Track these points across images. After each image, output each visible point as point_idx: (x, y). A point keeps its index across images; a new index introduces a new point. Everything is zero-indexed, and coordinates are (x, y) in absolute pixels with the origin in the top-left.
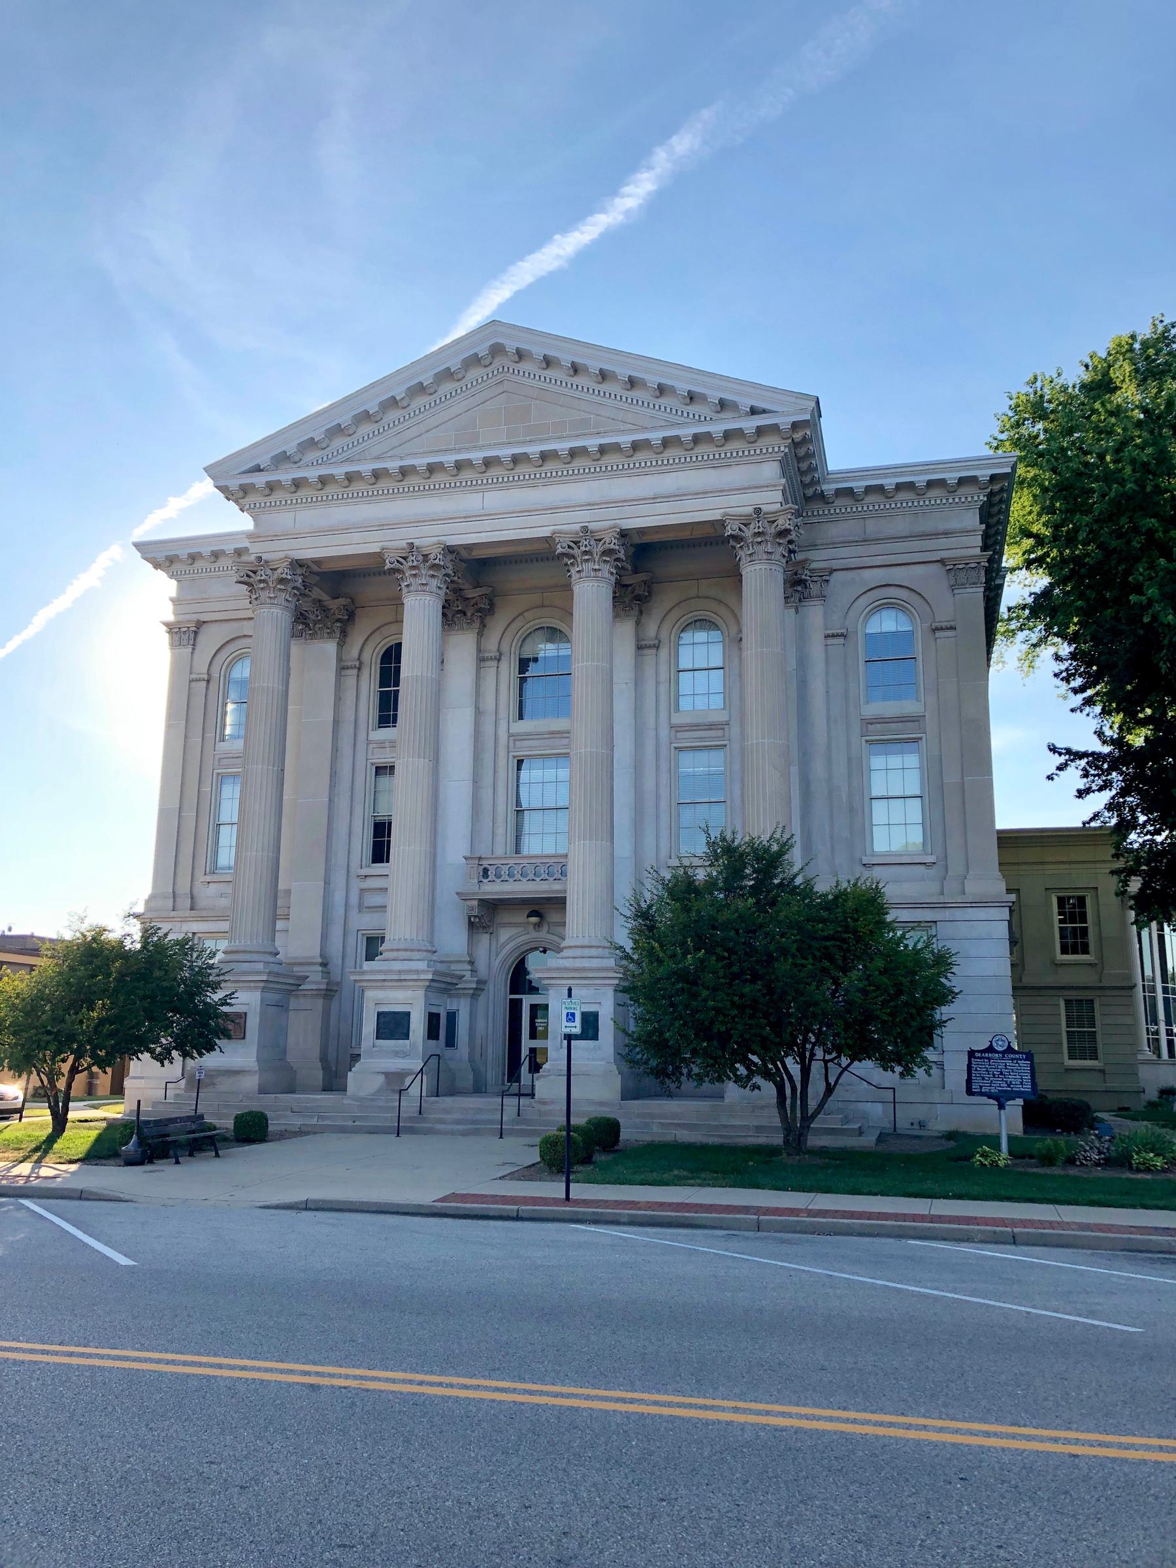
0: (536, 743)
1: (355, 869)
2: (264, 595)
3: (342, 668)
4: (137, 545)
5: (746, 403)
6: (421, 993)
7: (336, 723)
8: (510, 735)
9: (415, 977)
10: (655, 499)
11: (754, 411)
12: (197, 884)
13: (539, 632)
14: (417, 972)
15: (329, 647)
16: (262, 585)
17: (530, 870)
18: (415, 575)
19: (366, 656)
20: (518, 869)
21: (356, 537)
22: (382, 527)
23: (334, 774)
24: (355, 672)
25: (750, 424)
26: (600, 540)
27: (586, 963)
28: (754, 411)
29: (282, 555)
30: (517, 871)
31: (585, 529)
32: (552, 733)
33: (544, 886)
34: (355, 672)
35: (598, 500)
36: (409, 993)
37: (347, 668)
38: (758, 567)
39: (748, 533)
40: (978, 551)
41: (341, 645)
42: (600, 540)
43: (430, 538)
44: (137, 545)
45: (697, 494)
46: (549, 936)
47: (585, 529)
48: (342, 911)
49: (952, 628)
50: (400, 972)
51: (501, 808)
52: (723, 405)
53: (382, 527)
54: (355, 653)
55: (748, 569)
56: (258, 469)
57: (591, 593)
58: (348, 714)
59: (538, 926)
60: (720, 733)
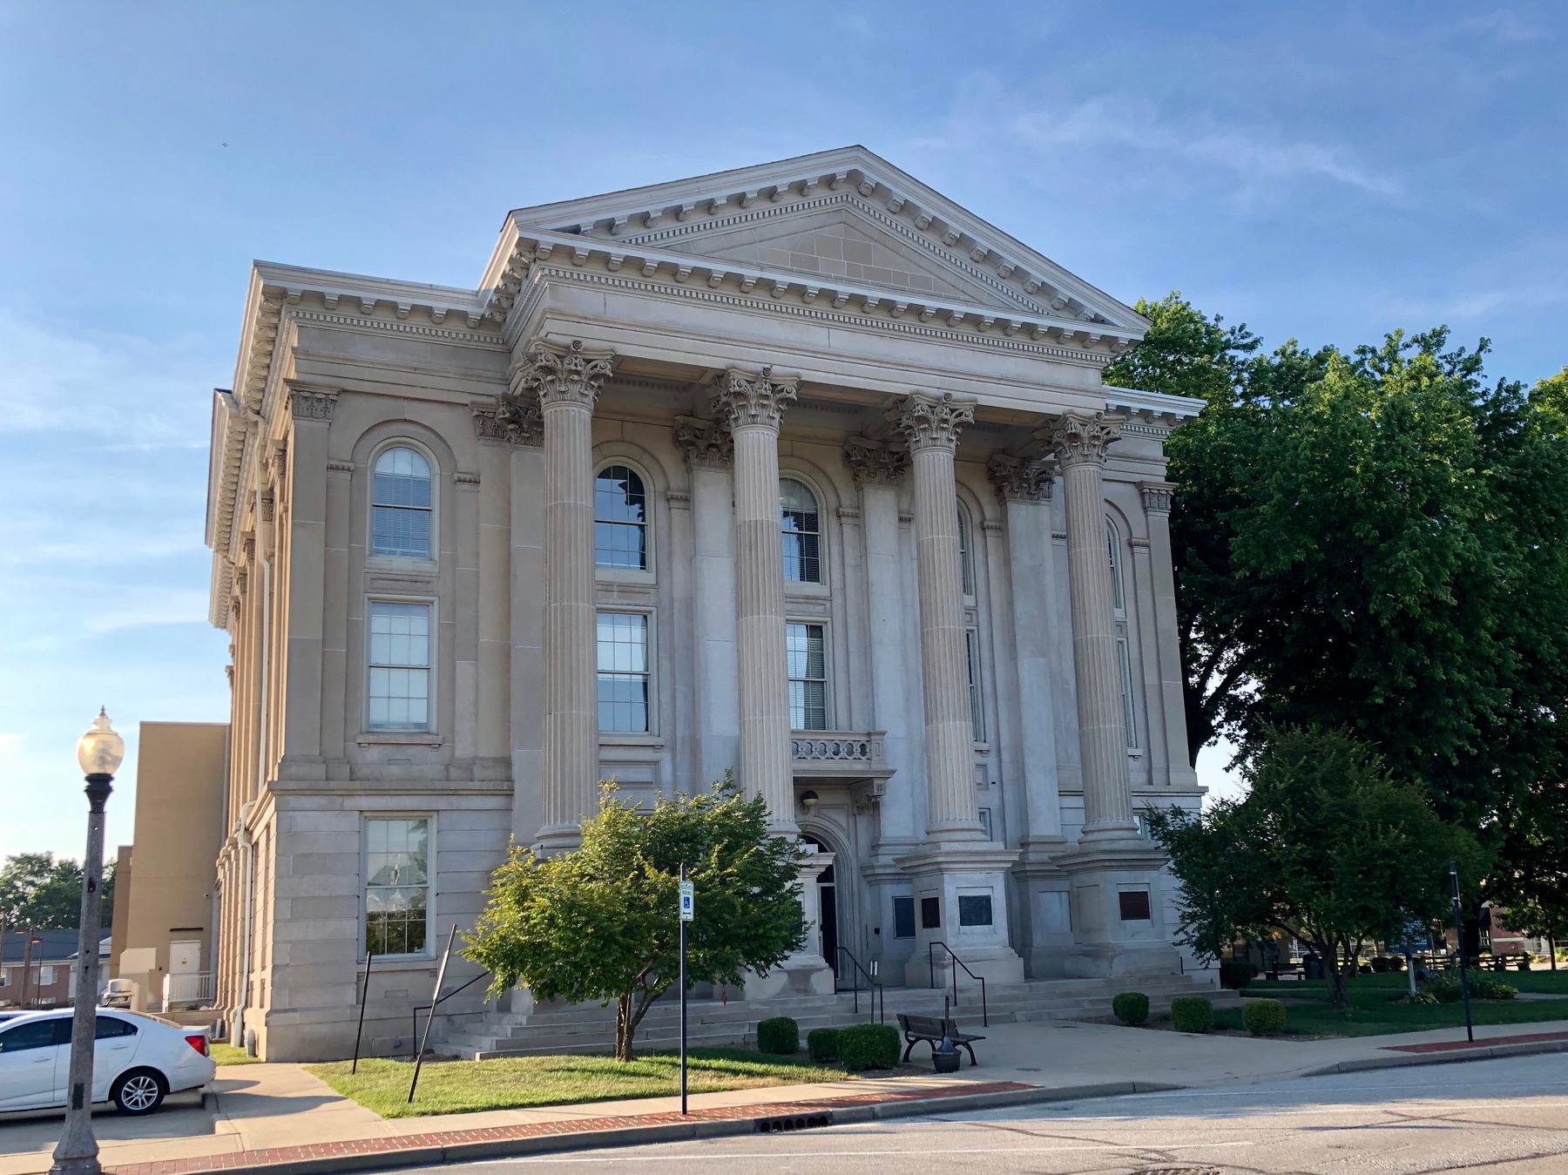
4: (257, 264)
5: (1092, 309)
10: (1001, 380)
11: (1098, 320)
12: (352, 745)
16: (576, 377)
17: (831, 748)
18: (763, 406)
20: (817, 746)
21: (687, 344)
22: (719, 339)
25: (1096, 331)
26: (953, 411)
28: (1098, 320)
29: (606, 345)
30: (817, 746)
31: (947, 396)
32: (807, 597)
33: (845, 765)
35: (949, 368)
40: (1162, 480)
42: (953, 411)
43: (793, 367)
44: (257, 264)
45: (1042, 385)
47: (947, 396)
49: (1147, 546)
51: (841, 678)
52: (1072, 308)
53: (719, 339)
56: (576, 230)
57: (935, 463)
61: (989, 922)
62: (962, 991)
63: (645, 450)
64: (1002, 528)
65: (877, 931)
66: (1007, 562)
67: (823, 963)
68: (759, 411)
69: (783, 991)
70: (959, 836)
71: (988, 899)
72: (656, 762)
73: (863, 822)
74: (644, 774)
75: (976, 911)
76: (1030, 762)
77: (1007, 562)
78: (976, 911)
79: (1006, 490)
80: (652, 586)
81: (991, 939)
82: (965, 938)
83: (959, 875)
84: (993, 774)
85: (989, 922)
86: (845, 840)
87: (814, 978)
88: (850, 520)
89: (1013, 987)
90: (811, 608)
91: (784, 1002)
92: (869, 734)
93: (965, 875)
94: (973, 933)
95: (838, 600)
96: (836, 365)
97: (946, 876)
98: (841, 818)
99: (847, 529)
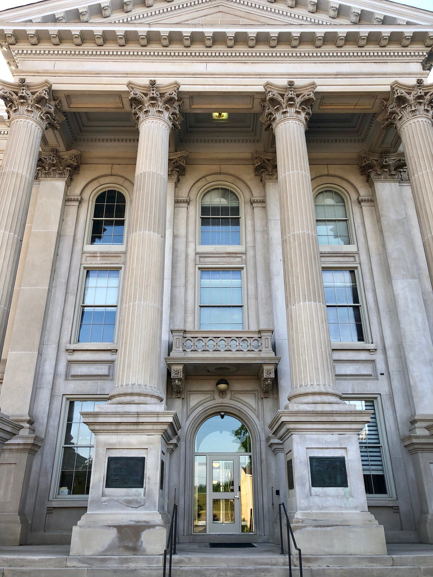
0: (216, 260)
1: (65, 344)
2: (22, 109)
3: (67, 200)
6: (157, 438)
7: (60, 236)
8: (197, 254)
9: (154, 420)
13: (216, 192)
14: (158, 414)
15: (60, 184)
19: (86, 195)
21: (105, 80)
23: (54, 270)
24: (77, 204)
27: (327, 408)
34: (77, 204)
36: (144, 438)
37: (71, 200)
38: (420, 119)
39: (411, 98)
41: (68, 185)
46: (232, 402)
48: (51, 377)
50: (138, 414)
54: (77, 191)
55: (411, 122)
58: (69, 231)
59: (222, 393)
60: (352, 259)
61: (344, 483)
62: (308, 560)
63: (126, 179)
64: (372, 200)
65: (278, 492)
66: (378, 220)
67: (158, 518)
68: (150, 109)
69: (110, 549)
70: (310, 399)
71: (341, 461)
72: (112, 362)
73: (268, 403)
74: (103, 370)
75: (329, 472)
76: (411, 356)
77: (378, 220)
78: (329, 472)
79: (372, 175)
80: (122, 253)
81: (350, 500)
82: (317, 499)
83: (309, 436)
84: (381, 367)
85: (344, 483)
86: (254, 417)
87: (145, 536)
88: (259, 205)
89: (371, 560)
90: (232, 260)
91: (103, 561)
92: (259, 332)
93: (315, 436)
94: (326, 495)
95: (250, 253)
96: (210, 81)
97: (296, 437)
98: (251, 401)
99: (256, 210)
